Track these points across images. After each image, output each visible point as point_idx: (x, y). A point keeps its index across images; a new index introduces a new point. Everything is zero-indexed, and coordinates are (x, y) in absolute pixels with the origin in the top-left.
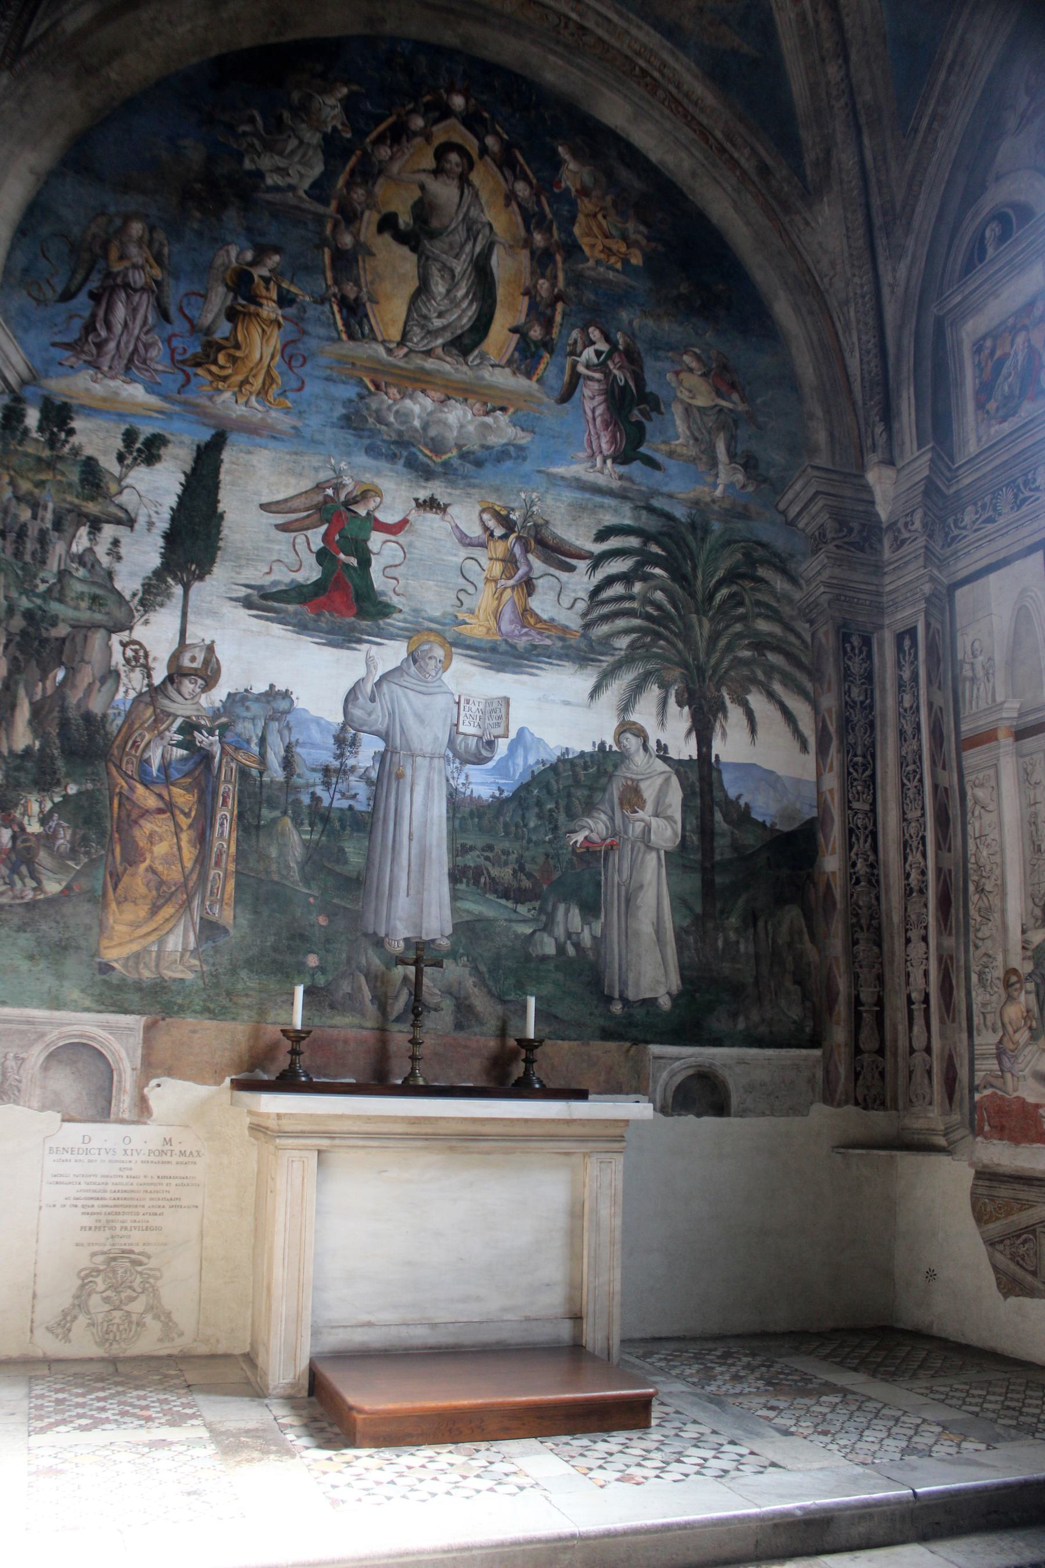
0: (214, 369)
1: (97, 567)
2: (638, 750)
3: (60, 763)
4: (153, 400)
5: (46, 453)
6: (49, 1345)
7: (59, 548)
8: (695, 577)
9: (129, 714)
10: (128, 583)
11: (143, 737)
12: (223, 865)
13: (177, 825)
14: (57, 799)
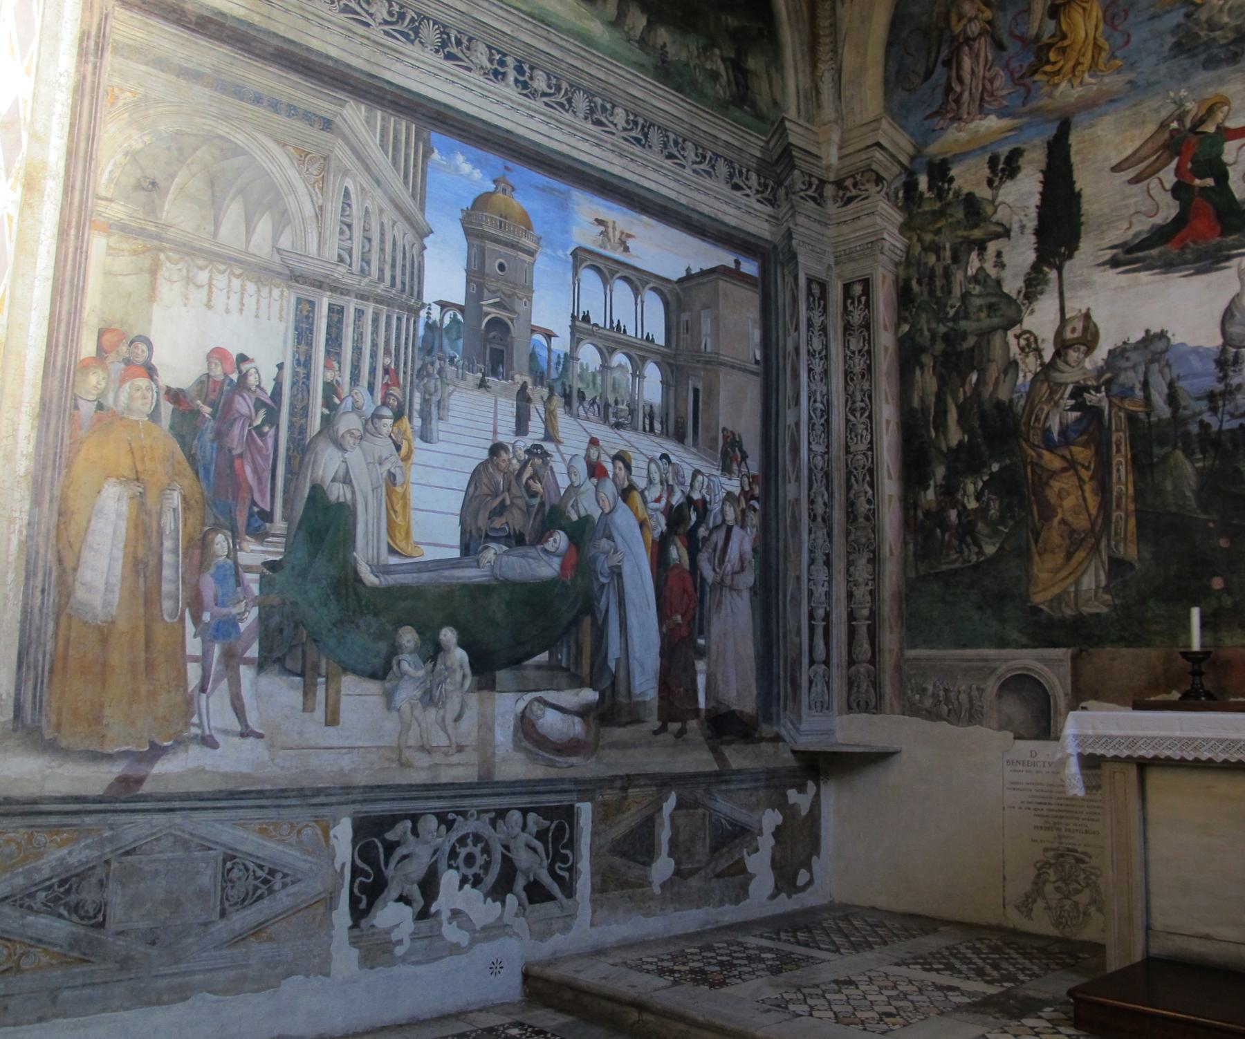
0: (1048, 68)
1: (989, 281)
3: (984, 448)
4: (1005, 123)
5: (937, 206)
6: (1016, 920)
7: (959, 276)
9: (1029, 394)
10: (1013, 285)
11: (1042, 410)
12: (1123, 506)
13: (1080, 479)
14: (986, 478)
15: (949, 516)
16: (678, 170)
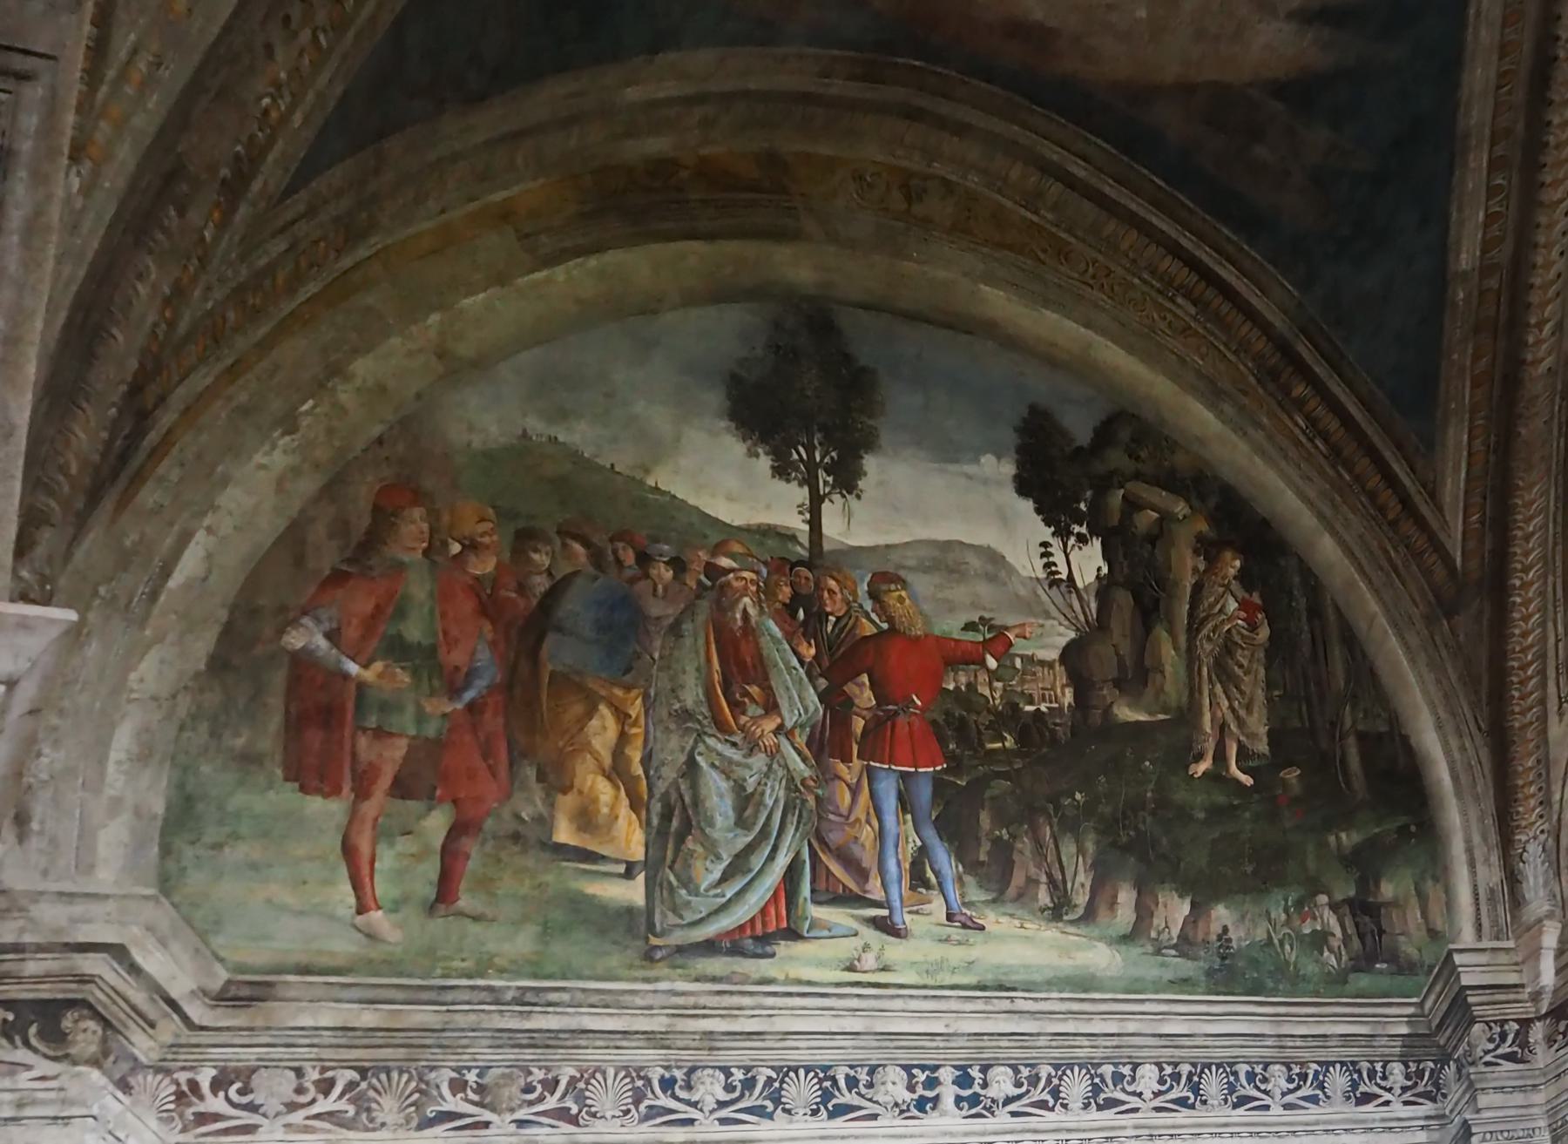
16: (1257, 1117)
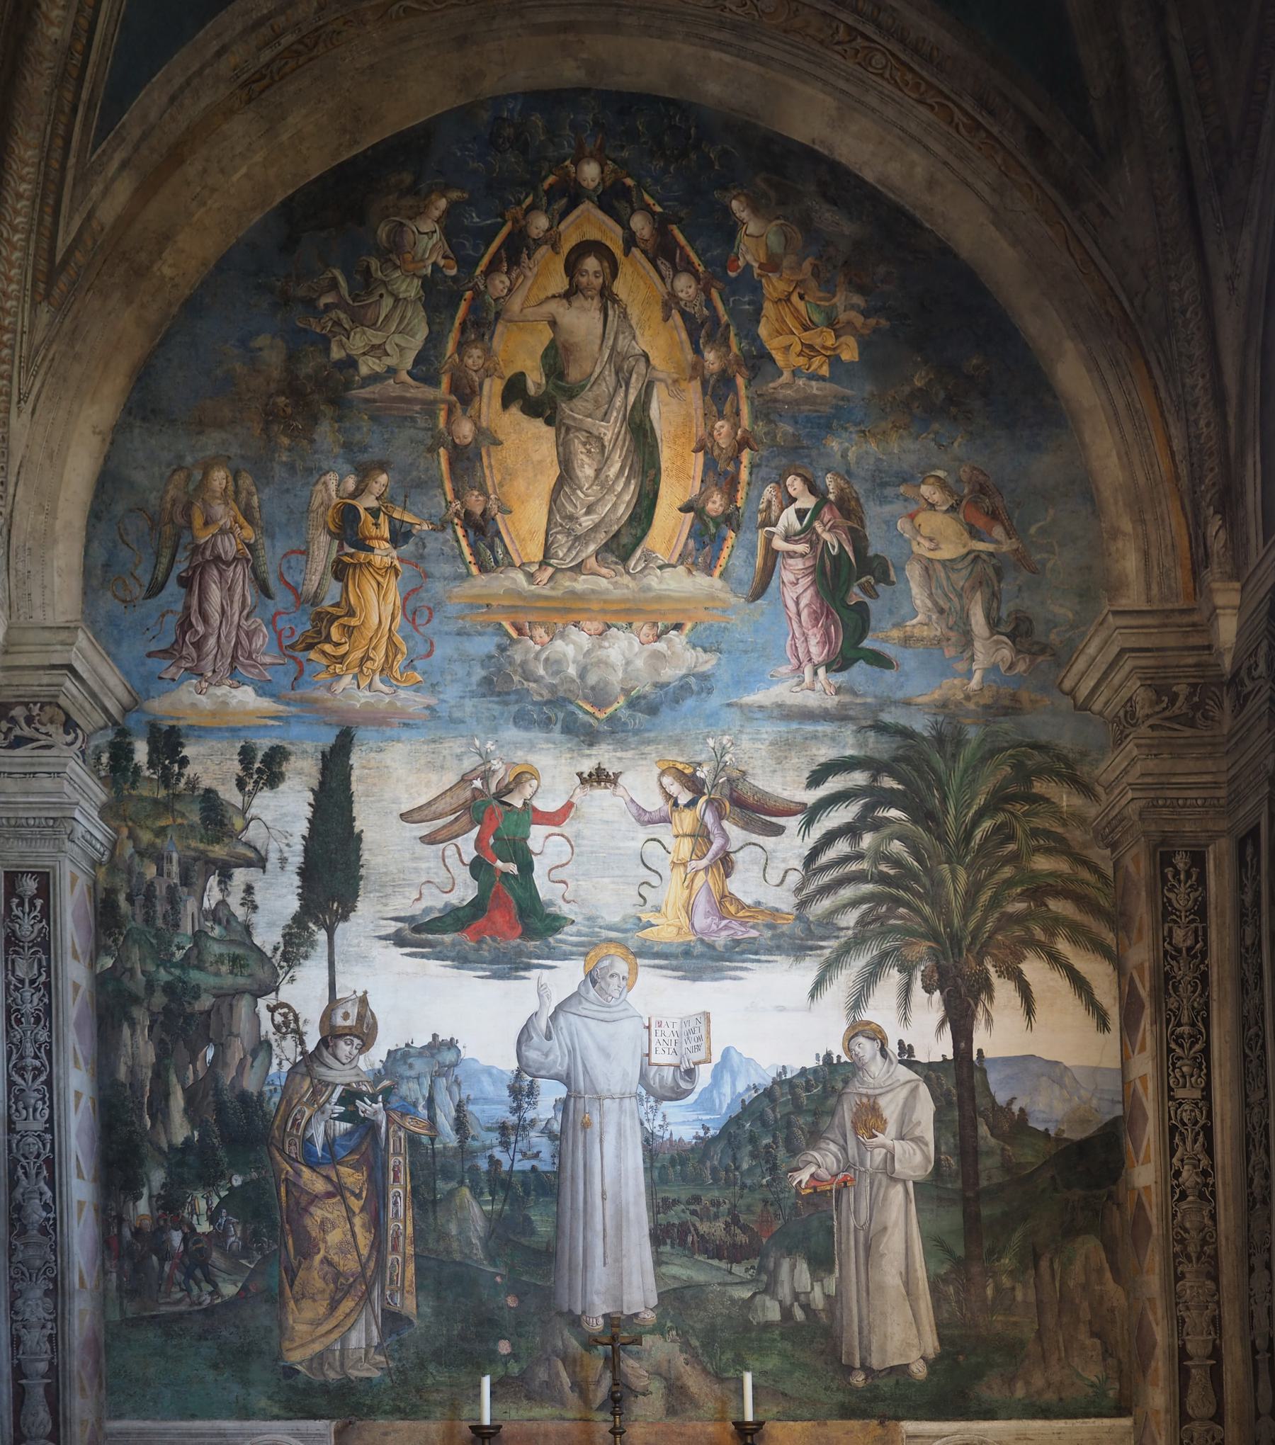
2: (874, 1058)
3: (221, 1153)
8: (946, 812)
9: (285, 1089)
14: (223, 1194)
15: (170, 1240)
